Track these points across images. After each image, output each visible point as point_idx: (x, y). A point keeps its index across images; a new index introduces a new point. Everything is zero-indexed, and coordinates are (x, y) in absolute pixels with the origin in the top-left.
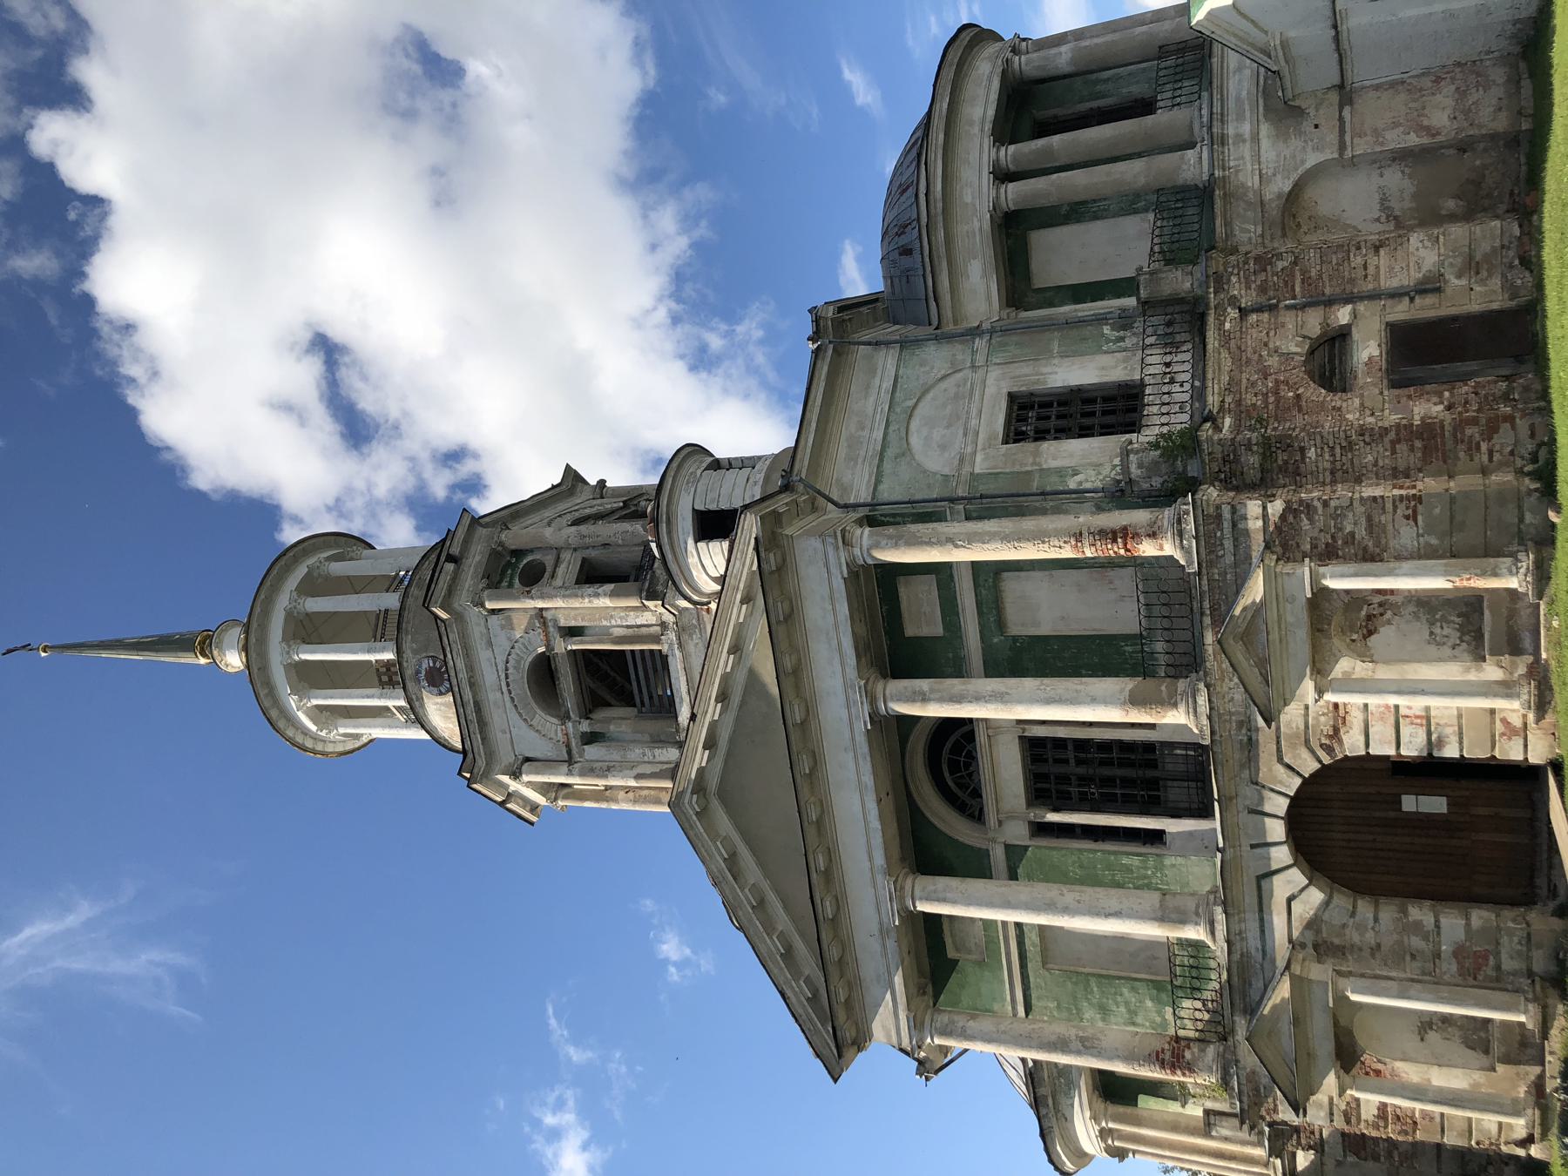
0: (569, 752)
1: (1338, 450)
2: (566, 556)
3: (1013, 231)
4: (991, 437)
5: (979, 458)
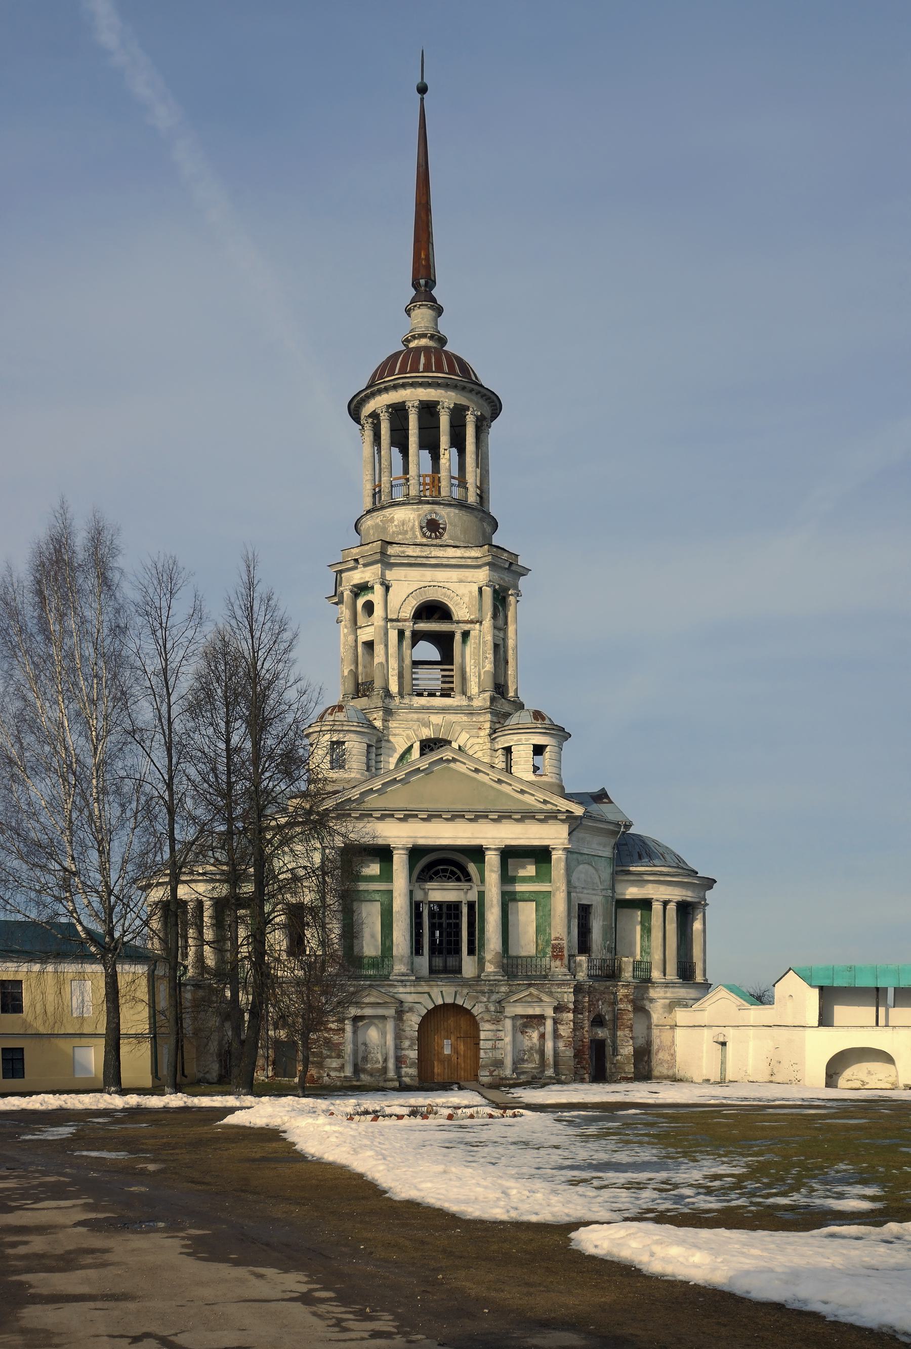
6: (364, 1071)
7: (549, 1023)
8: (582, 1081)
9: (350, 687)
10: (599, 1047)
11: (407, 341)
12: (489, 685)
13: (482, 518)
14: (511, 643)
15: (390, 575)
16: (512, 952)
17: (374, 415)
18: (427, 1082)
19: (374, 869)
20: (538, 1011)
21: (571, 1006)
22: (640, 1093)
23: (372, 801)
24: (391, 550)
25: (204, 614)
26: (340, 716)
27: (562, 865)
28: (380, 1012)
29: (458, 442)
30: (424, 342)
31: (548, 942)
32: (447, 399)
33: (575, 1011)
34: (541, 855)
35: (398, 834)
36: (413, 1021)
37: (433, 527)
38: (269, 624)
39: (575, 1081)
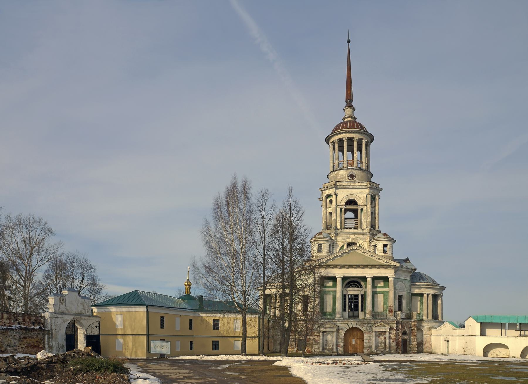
3: (421, 295)
6: (326, 349)
7: (387, 334)
8: (399, 353)
9: (325, 226)
10: (405, 342)
11: (344, 119)
12: (369, 225)
13: (368, 173)
14: (377, 212)
15: (337, 191)
16: (375, 311)
17: (333, 142)
18: (346, 353)
19: (331, 284)
20: (384, 330)
21: (395, 328)
22: (415, 357)
23: (330, 263)
24: (338, 184)
25: (276, 206)
26: (321, 236)
27: (392, 282)
28: (332, 330)
29: (360, 149)
30: (349, 119)
31: (387, 307)
32: (356, 136)
33: (396, 330)
34: (385, 279)
35: (339, 273)
36: (342, 333)
37: (352, 176)
38: (296, 209)
39: (396, 353)
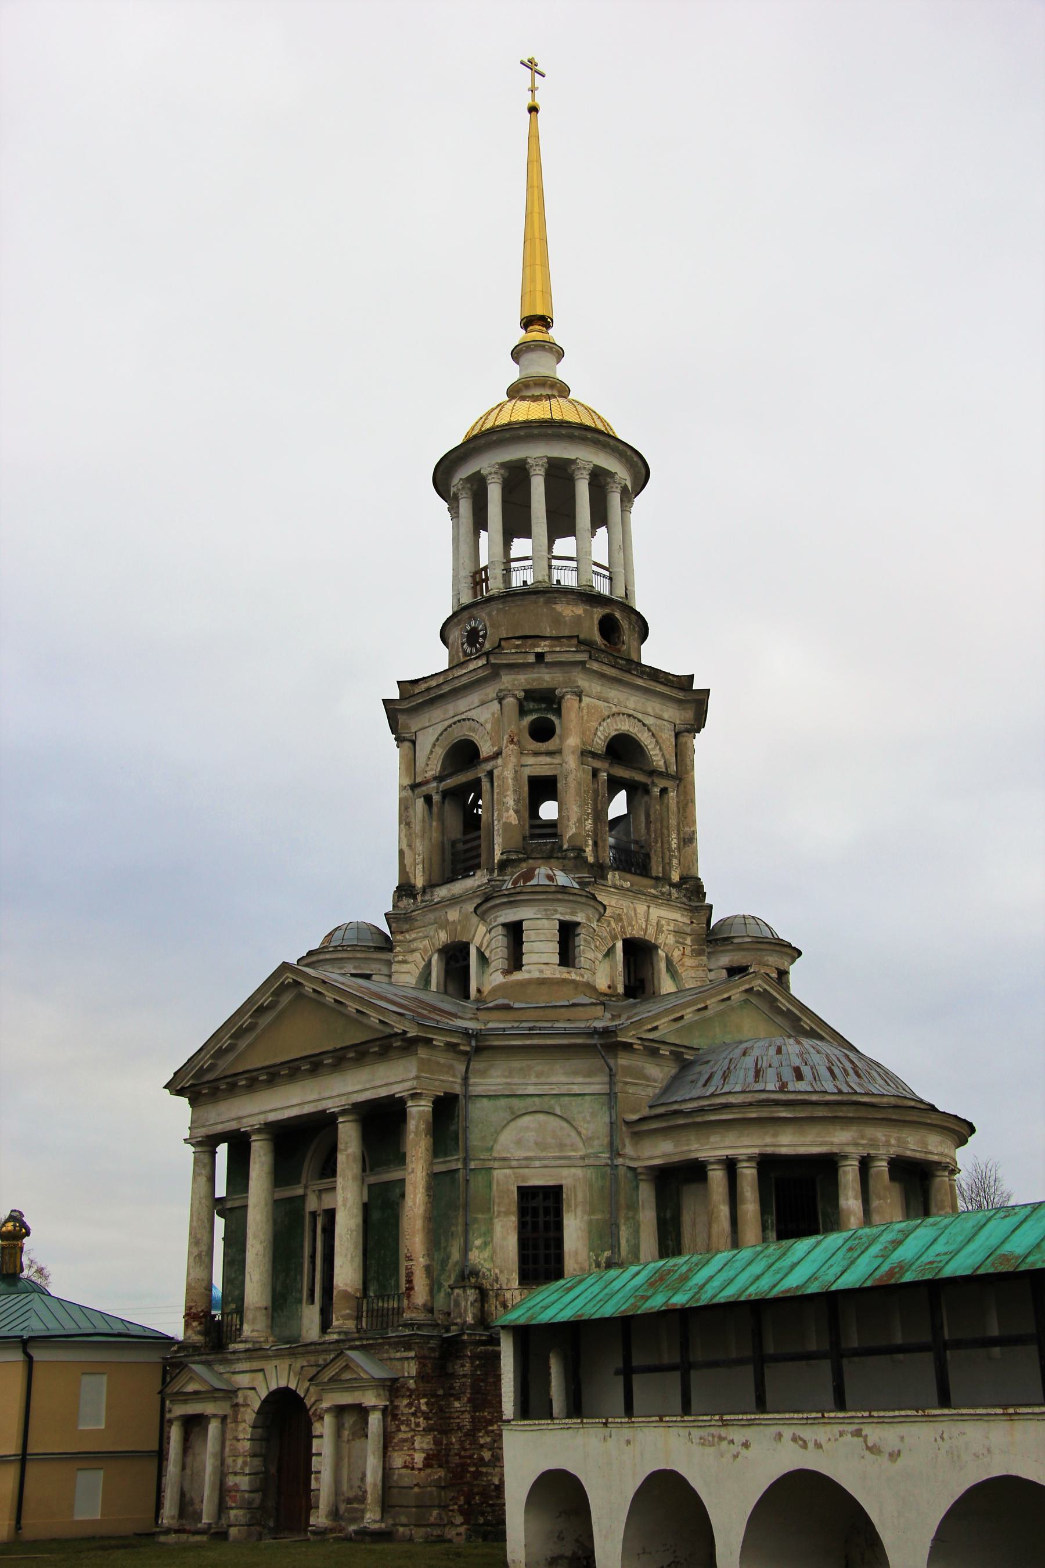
0: (420, 785)
1: (458, 1421)
2: (557, 760)
4: (524, 1178)
5: (507, 1171)
